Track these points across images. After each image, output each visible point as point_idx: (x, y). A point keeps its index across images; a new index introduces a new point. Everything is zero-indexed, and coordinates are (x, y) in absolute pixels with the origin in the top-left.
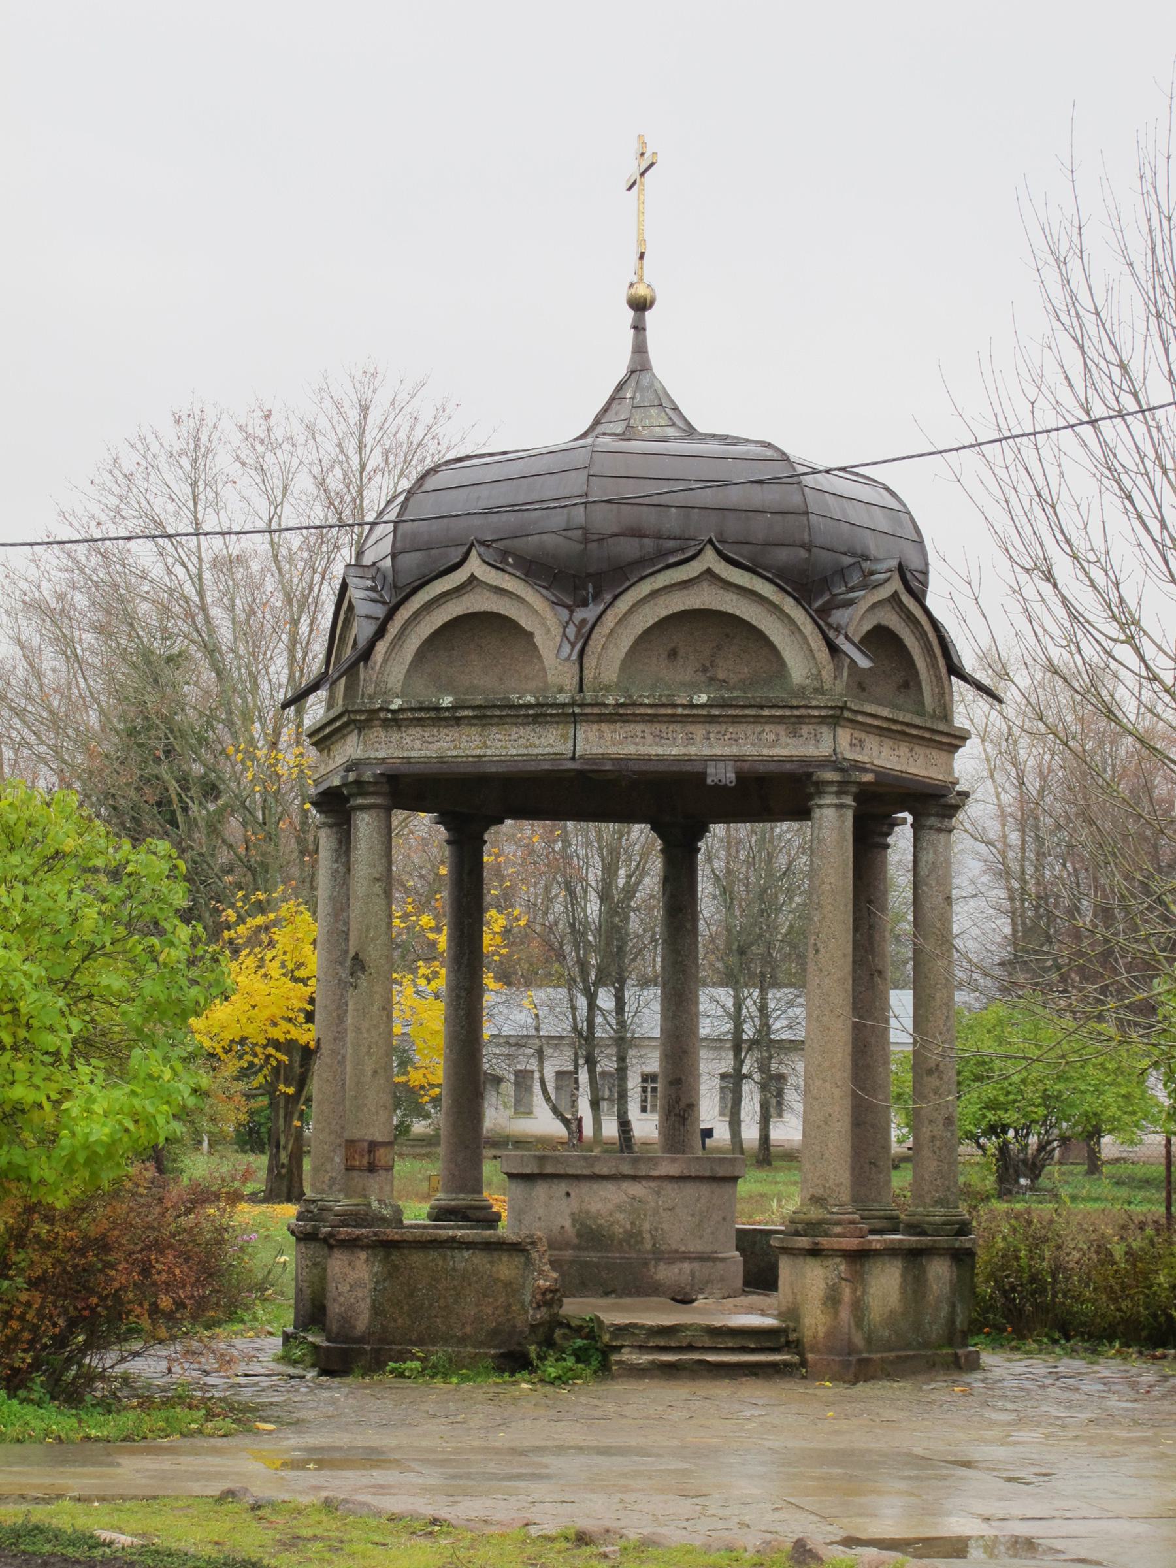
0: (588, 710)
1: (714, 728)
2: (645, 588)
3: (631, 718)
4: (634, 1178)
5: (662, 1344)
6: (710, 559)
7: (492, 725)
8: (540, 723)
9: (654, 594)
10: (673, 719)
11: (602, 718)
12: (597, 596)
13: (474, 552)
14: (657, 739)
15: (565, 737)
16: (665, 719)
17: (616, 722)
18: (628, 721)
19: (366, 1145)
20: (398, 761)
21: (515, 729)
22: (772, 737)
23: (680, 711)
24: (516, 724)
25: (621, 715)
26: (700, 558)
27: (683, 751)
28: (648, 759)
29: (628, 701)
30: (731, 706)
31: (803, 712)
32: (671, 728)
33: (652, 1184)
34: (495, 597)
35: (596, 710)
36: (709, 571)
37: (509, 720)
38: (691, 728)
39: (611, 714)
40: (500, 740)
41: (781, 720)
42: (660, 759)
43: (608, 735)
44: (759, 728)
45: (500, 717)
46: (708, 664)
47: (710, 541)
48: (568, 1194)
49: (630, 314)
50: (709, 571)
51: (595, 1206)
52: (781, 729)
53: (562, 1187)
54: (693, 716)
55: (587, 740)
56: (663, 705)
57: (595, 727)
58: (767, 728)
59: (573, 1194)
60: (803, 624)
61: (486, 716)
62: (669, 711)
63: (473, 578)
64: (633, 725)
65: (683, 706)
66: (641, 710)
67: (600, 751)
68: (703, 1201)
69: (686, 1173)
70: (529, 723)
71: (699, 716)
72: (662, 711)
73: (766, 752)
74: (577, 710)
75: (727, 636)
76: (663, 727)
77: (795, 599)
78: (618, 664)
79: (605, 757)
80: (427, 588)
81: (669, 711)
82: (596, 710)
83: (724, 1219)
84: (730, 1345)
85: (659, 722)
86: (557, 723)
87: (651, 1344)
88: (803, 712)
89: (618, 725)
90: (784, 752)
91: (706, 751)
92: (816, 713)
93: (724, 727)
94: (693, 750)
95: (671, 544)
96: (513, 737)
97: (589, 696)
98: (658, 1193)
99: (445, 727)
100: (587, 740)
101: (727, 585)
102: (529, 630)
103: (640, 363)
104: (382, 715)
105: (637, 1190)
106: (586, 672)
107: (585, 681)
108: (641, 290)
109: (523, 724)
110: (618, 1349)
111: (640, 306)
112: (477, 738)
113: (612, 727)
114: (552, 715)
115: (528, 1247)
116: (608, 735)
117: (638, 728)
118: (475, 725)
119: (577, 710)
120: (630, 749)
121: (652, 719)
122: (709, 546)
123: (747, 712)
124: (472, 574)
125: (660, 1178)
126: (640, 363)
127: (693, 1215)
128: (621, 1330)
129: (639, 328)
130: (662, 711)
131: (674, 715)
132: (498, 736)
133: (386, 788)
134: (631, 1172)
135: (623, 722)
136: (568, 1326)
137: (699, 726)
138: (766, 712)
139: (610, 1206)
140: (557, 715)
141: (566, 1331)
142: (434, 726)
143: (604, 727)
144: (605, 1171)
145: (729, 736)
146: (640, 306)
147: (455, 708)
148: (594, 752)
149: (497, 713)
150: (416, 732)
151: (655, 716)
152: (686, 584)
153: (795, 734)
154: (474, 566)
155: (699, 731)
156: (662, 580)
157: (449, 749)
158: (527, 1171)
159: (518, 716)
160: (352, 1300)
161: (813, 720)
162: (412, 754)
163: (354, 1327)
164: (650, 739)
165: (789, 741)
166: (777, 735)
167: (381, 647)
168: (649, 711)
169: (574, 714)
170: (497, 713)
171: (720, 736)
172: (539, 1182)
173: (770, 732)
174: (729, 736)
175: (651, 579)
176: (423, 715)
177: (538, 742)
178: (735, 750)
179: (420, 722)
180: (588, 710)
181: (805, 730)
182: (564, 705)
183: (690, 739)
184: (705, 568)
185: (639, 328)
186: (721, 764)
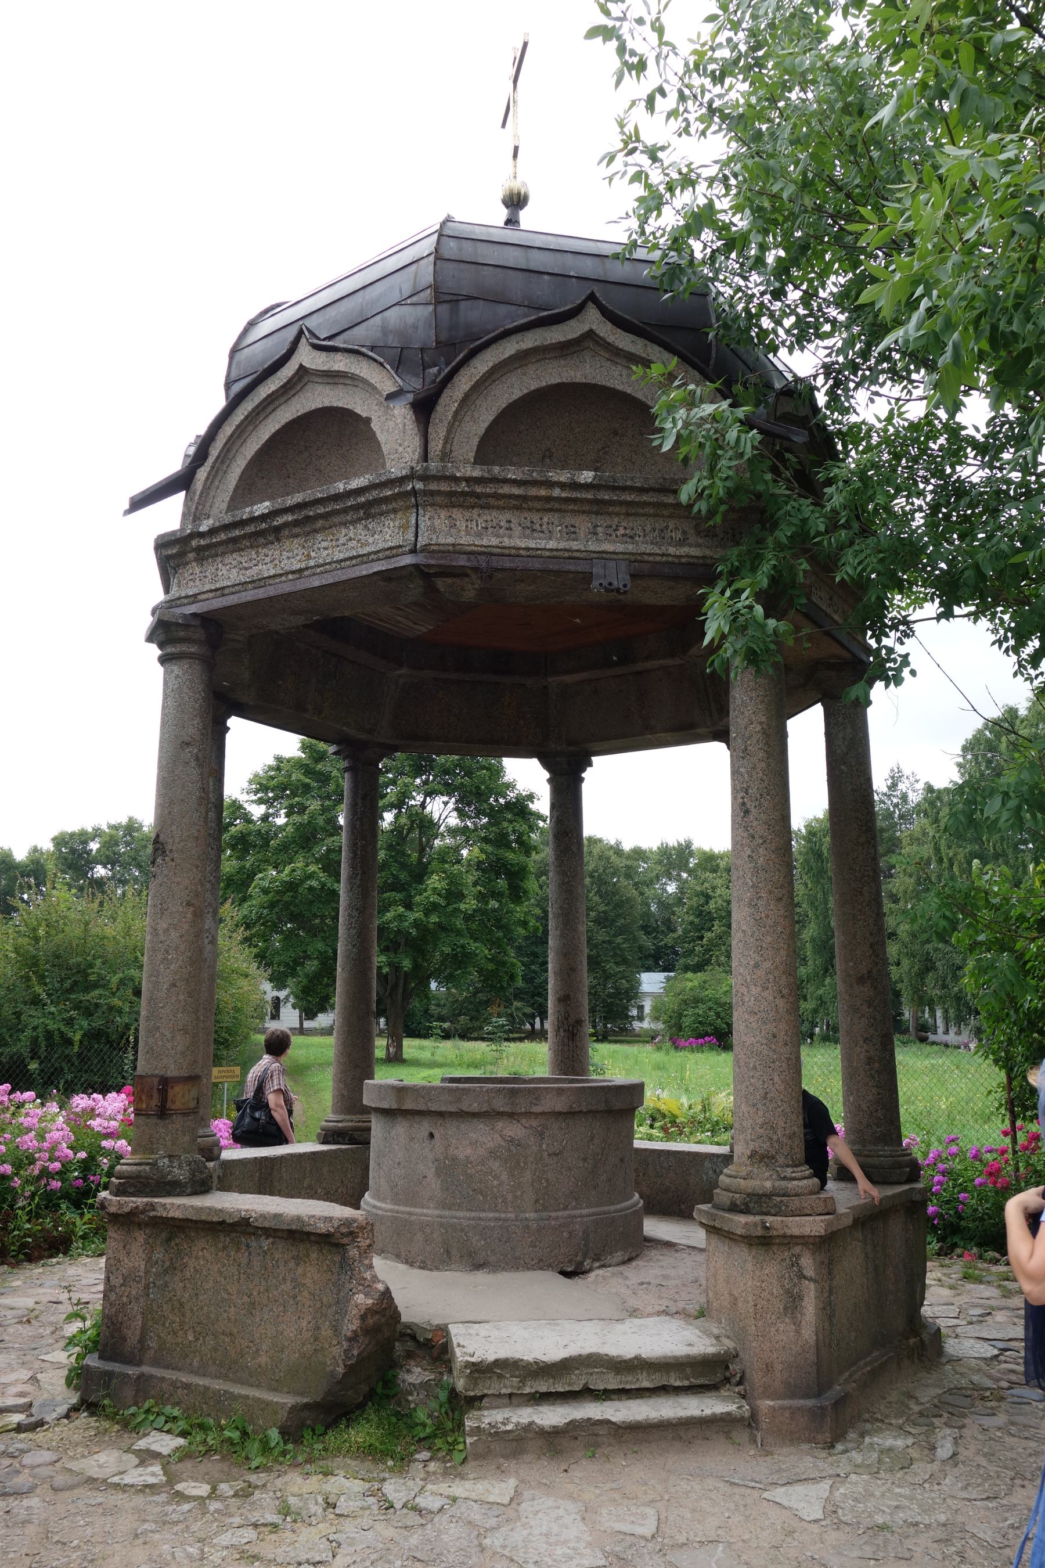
0: (433, 486)
1: (602, 521)
4: (512, 1115)
5: (544, 1389)
6: (592, 320)
7: (316, 531)
8: (374, 517)
9: (522, 358)
10: (549, 505)
13: (303, 340)
14: (528, 532)
15: (404, 527)
16: (538, 505)
18: (488, 507)
19: (156, 1081)
20: (211, 595)
21: (344, 531)
23: (557, 492)
24: (344, 524)
25: (478, 496)
27: (562, 545)
28: (515, 553)
29: (486, 475)
32: (545, 519)
33: (534, 1123)
36: (591, 331)
37: (336, 520)
38: (569, 520)
40: (325, 549)
43: (461, 524)
44: (660, 524)
45: (326, 516)
47: (592, 298)
48: (432, 1136)
50: (590, 334)
51: (464, 1152)
53: (425, 1127)
55: (433, 529)
57: (443, 514)
59: (437, 1135)
61: (308, 518)
62: (543, 492)
64: (495, 513)
65: (563, 486)
66: (506, 490)
67: (450, 540)
68: (596, 1141)
70: (360, 520)
71: (582, 501)
72: (533, 492)
73: (672, 550)
74: (419, 486)
75: (616, 433)
76: (536, 517)
78: (475, 441)
79: (456, 550)
80: (250, 396)
82: (444, 487)
83: (622, 1160)
84: (646, 1384)
86: (395, 511)
87: (527, 1390)
89: (475, 511)
91: (593, 546)
93: (616, 520)
94: (575, 545)
96: (342, 540)
97: (434, 466)
98: (541, 1134)
99: (265, 545)
100: (433, 529)
102: (364, 415)
104: (194, 543)
105: (514, 1130)
106: (431, 445)
108: (516, 185)
112: (300, 551)
113: (467, 514)
115: (345, 1241)
116: (461, 524)
117: (503, 517)
118: (297, 536)
119: (419, 486)
121: (520, 504)
123: (645, 498)
125: (543, 1113)
127: (585, 1160)
130: (533, 492)
131: (549, 499)
132: (324, 544)
133: (200, 634)
134: (507, 1109)
135: (482, 507)
136: (413, 1338)
137: (584, 517)
139: (481, 1151)
141: (410, 1345)
142: (252, 547)
143: (457, 513)
144: (475, 1107)
145: (622, 531)
148: (442, 541)
149: (321, 510)
150: (232, 559)
151: (525, 498)
155: (583, 524)
158: (386, 1106)
159: (345, 511)
160: (125, 1299)
164: (517, 531)
166: (684, 532)
167: (202, 474)
168: (516, 491)
169: (414, 492)
170: (321, 510)
171: (610, 531)
172: (399, 1119)
174: (622, 531)
178: (631, 548)
179: (234, 545)
180: (433, 486)
184: (586, 328)
186: (612, 564)
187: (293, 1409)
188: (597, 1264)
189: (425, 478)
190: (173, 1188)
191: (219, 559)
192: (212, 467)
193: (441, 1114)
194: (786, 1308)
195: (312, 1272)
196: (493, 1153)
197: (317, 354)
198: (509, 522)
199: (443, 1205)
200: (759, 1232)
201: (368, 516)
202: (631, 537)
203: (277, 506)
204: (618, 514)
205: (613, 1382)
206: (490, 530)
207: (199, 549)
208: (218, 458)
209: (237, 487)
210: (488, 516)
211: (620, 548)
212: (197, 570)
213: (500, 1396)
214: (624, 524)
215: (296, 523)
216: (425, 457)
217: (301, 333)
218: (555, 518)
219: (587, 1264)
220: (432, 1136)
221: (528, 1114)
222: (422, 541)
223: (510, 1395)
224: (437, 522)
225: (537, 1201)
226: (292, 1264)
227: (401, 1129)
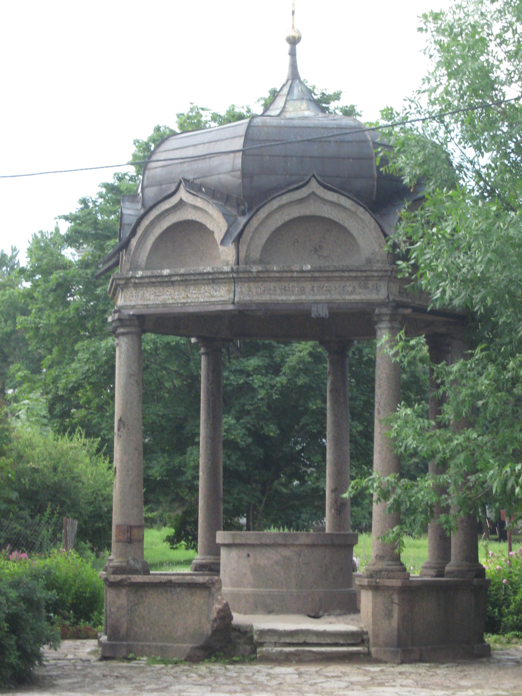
1: (316, 284)
2: (275, 204)
3: (267, 279)
4: (285, 545)
6: (314, 186)
8: (216, 283)
9: (281, 207)
11: (249, 280)
12: (250, 209)
13: (182, 186)
15: (229, 291)
17: (258, 281)
18: (265, 281)
21: (203, 287)
22: (350, 289)
23: (295, 274)
24: (204, 284)
25: (261, 278)
26: (308, 186)
27: (298, 298)
28: (277, 304)
29: (264, 270)
30: (326, 271)
31: (368, 274)
32: (291, 285)
33: (296, 549)
34: (193, 211)
35: (246, 275)
36: (313, 193)
38: (302, 284)
39: (254, 277)
40: (195, 294)
41: (356, 278)
42: (285, 303)
44: (343, 284)
45: (195, 280)
46: (317, 247)
47: (314, 176)
48: (249, 555)
49: (288, 46)
50: (313, 193)
52: (356, 284)
54: (304, 277)
56: (285, 271)
57: (246, 285)
58: (348, 284)
59: (251, 555)
60: (369, 223)
62: (289, 275)
63: (181, 202)
64: (268, 284)
65: (297, 272)
66: (273, 275)
69: (315, 542)
70: (210, 284)
72: (285, 275)
73: (347, 297)
74: (235, 275)
75: (328, 230)
76: (286, 284)
77: (364, 208)
78: (260, 248)
79: (251, 302)
80: (157, 207)
81: (289, 275)
82: (246, 275)
85: (284, 281)
86: (225, 283)
87: (282, 641)
88: (368, 274)
90: (356, 297)
91: (311, 298)
92: (376, 274)
93: (323, 283)
94: (303, 297)
95: (294, 178)
96: (202, 291)
97: (242, 266)
101: (324, 201)
102: (211, 229)
103: (294, 75)
105: (287, 552)
106: (240, 254)
107: (240, 258)
109: (207, 284)
110: (262, 644)
111: (294, 41)
112: (183, 292)
113: (256, 285)
114: (222, 279)
115: (210, 586)
116: (254, 290)
117: (272, 285)
118: (182, 285)
120: (266, 298)
121: (280, 279)
122: (313, 179)
124: (181, 199)
126: (294, 75)
127: (321, 567)
128: (262, 633)
129: (293, 54)
130: (285, 275)
131: (292, 277)
132: (194, 292)
133: (136, 322)
134: (283, 542)
135: (263, 281)
136: (239, 631)
138: (346, 274)
140: (225, 278)
141: (238, 633)
143: (252, 285)
144: (268, 541)
145: (325, 288)
146: (294, 41)
147: (170, 276)
148: (245, 299)
149: (193, 278)
150: (151, 290)
152: (301, 201)
153: (366, 287)
154: (183, 194)
155: (308, 286)
156: (285, 199)
157: (169, 299)
161: (375, 278)
162: (149, 303)
163: (119, 632)
164: (278, 291)
165: (361, 291)
166: (354, 287)
167: (134, 242)
168: (277, 275)
169: (233, 278)
170: (193, 278)
172: (234, 548)
173: (349, 286)
175: (278, 199)
176: (154, 280)
177: (215, 294)
178: (328, 297)
179: (153, 284)
180: (241, 275)
181: (370, 284)
182: (227, 273)
183: (302, 291)
184: (310, 191)
185: (293, 54)
187: (192, 648)
188: (326, 614)
189: (237, 272)
190: (136, 572)
191: (145, 288)
192: (139, 239)
193: (253, 545)
194: (385, 615)
195: (199, 599)
196: (277, 563)
197: (188, 194)
198: (275, 287)
199: (254, 586)
200: (374, 584)
201: (213, 283)
202: (329, 291)
203: (173, 273)
204: (323, 281)
205: (315, 640)
206: (266, 292)
207: (135, 283)
208: (141, 235)
209: (151, 249)
210: (267, 285)
211: (323, 297)
212: (134, 292)
213: (271, 643)
214: (326, 285)
215: (182, 281)
216: (238, 262)
217: (181, 182)
218: (295, 284)
219: (321, 613)
220: (249, 555)
221: (293, 545)
222: (236, 299)
223: (275, 643)
224: (243, 289)
225: (297, 584)
226: (189, 597)
227: (234, 553)
